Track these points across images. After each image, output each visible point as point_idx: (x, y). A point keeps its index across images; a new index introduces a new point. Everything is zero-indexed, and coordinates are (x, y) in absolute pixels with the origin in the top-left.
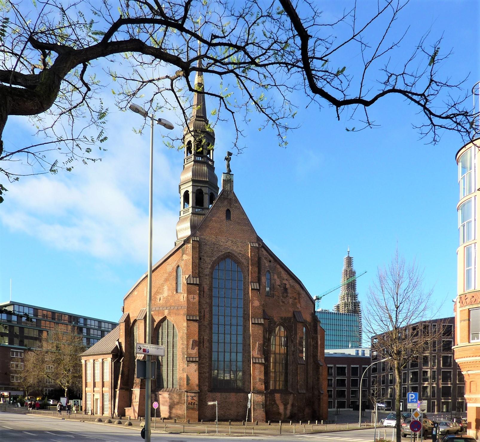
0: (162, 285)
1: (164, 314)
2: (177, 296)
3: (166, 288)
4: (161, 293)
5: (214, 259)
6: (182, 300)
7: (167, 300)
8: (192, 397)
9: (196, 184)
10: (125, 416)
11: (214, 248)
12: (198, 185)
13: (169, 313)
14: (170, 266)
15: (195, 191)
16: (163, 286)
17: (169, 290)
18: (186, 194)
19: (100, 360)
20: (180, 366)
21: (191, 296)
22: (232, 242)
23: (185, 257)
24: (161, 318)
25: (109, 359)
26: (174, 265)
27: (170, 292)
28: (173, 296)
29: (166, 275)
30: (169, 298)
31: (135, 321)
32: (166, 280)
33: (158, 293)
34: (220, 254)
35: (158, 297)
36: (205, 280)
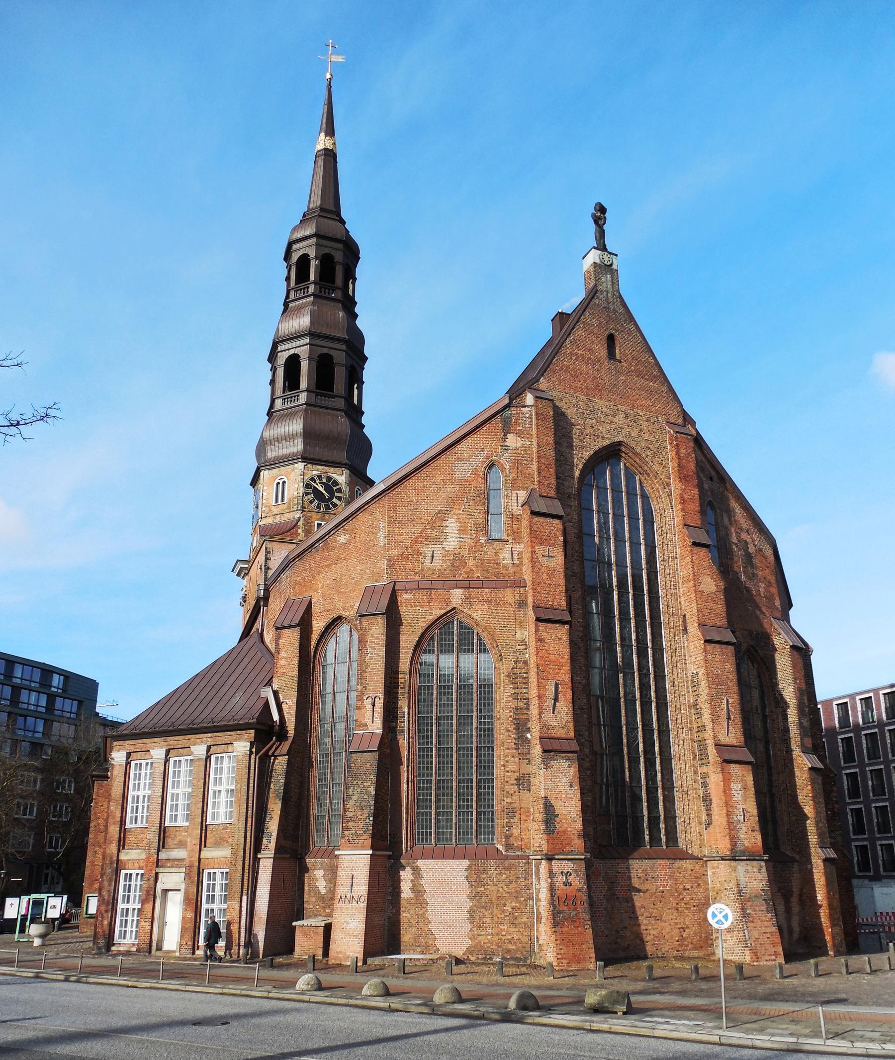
0: (441, 516)
1: (447, 601)
2: (489, 551)
3: (452, 525)
4: (438, 541)
6: (508, 562)
7: (457, 561)
8: (568, 874)
9: (318, 342)
10: (290, 950)
12: (322, 343)
13: (468, 600)
14: (468, 462)
15: (315, 356)
16: (444, 520)
17: (462, 530)
18: (293, 363)
19: (199, 750)
20: (510, 767)
21: (540, 550)
22: (627, 417)
24: (438, 612)
25: (242, 745)
27: (467, 537)
28: (476, 548)
30: (466, 553)
31: (337, 621)
32: (453, 502)
33: (427, 538)
35: (427, 551)
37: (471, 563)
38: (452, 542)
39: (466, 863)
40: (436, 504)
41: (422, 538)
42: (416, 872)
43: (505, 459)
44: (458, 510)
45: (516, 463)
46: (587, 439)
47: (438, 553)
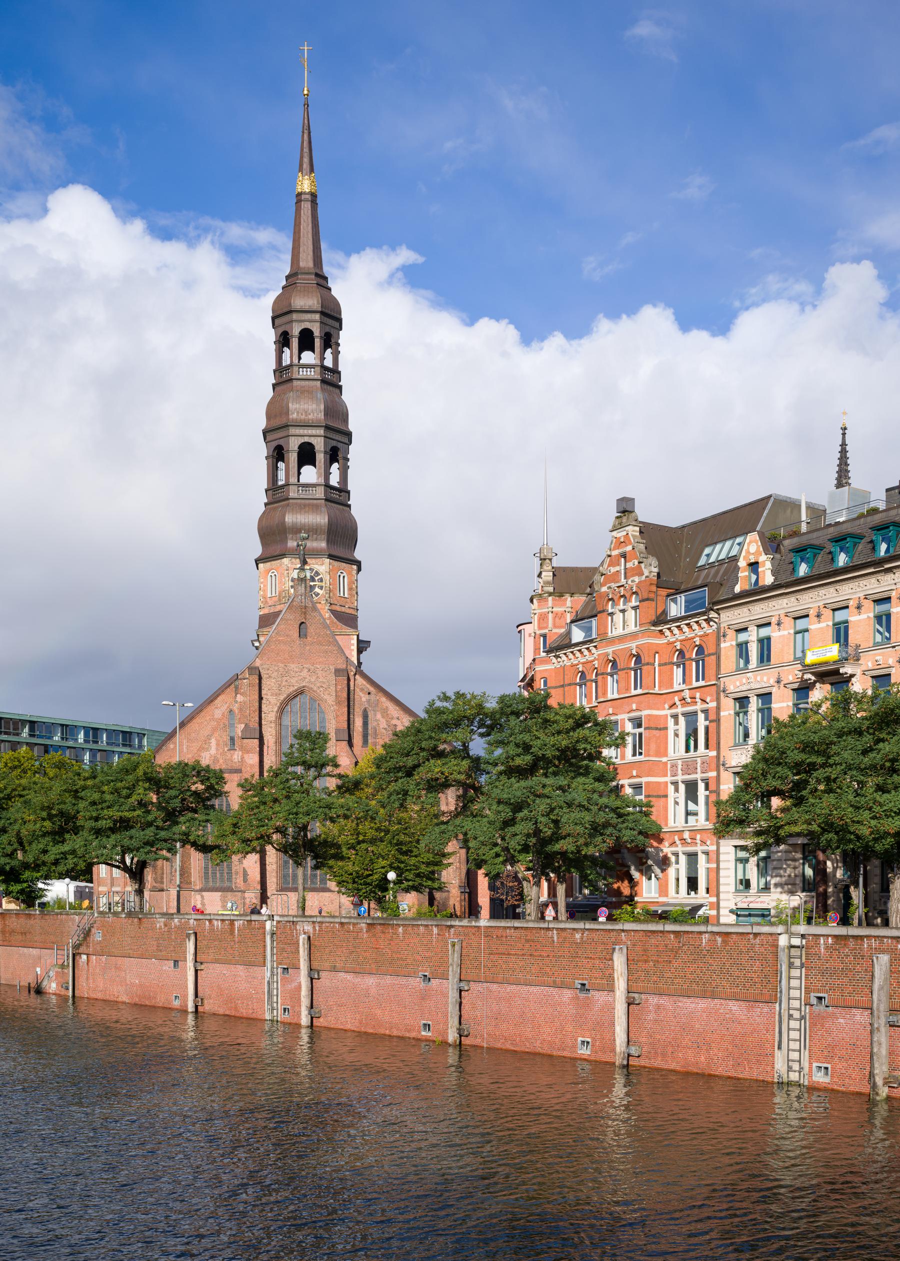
0: (209, 737)
3: (213, 742)
4: (207, 750)
5: (282, 698)
11: (282, 682)
17: (218, 745)
23: (239, 698)
26: (224, 708)
29: (214, 723)
32: (214, 730)
34: (292, 689)
36: (270, 729)
37: (221, 761)
38: (213, 751)
39: (220, 893)
40: (206, 732)
41: (201, 749)
42: (202, 897)
43: (236, 708)
44: (216, 734)
45: (240, 710)
46: (283, 689)
47: (208, 756)
